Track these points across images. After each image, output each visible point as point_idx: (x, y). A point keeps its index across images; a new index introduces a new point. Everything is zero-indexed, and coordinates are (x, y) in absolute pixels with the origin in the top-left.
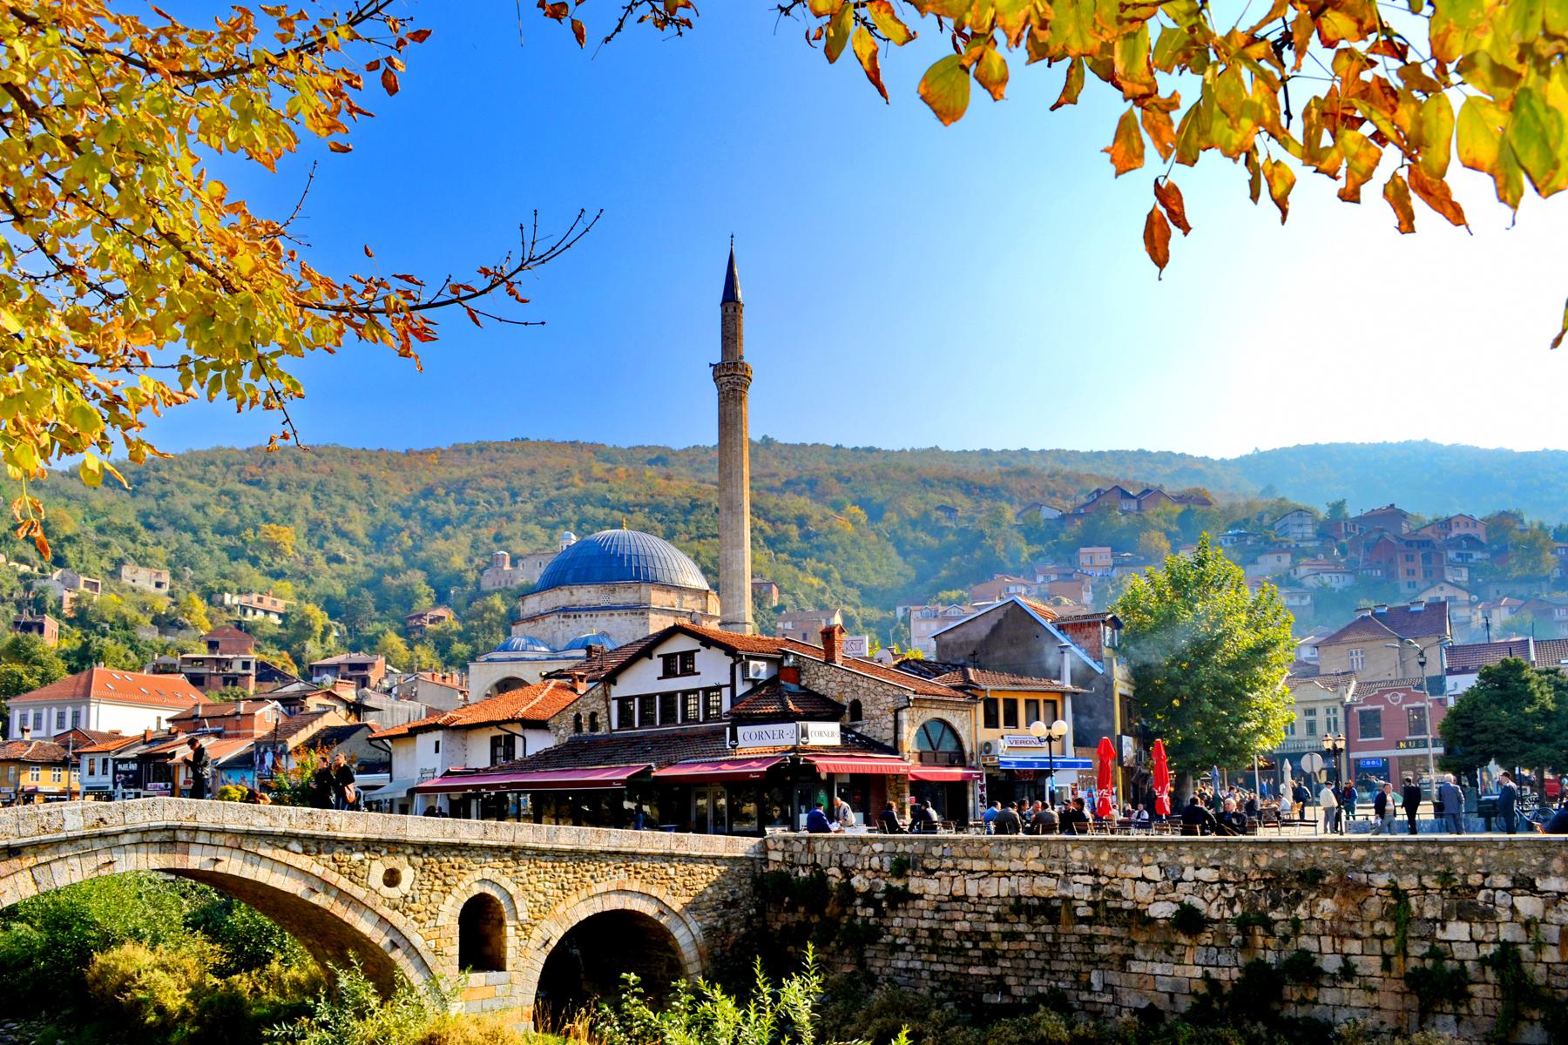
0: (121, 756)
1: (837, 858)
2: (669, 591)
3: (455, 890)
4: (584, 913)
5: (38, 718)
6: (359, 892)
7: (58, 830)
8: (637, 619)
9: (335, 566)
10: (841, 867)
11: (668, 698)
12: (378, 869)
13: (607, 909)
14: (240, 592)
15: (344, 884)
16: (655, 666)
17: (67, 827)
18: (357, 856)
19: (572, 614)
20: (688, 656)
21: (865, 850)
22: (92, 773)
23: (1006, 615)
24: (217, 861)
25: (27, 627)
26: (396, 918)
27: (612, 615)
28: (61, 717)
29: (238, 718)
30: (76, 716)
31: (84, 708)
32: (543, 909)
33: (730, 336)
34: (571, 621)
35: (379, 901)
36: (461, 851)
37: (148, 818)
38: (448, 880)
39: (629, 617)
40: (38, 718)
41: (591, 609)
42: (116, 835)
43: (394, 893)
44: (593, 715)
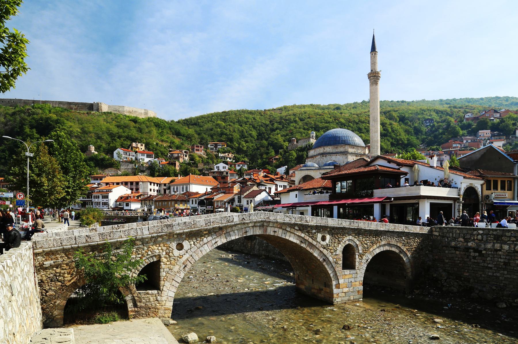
1: (462, 235)
2: (354, 148)
3: (341, 243)
4: (378, 251)
6: (314, 243)
7: (232, 222)
8: (344, 157)
10: (464, 238)
13: (384, 250)
15: (310, 240)
17: (234, 221)
18: (314, 231)
19: (324, 155)
21: (475, 232)
22: (192, 203)
24: (275, 232)
26: (325, 251)
32: (366, 250)
33: (373, 63)
34: (324, 158)
35: (320, 246)
36: (343, 230)
37: (256, 218)
38: (340, 239)
39: (342, 156)
42: (248, 224)
43: (323, 243)
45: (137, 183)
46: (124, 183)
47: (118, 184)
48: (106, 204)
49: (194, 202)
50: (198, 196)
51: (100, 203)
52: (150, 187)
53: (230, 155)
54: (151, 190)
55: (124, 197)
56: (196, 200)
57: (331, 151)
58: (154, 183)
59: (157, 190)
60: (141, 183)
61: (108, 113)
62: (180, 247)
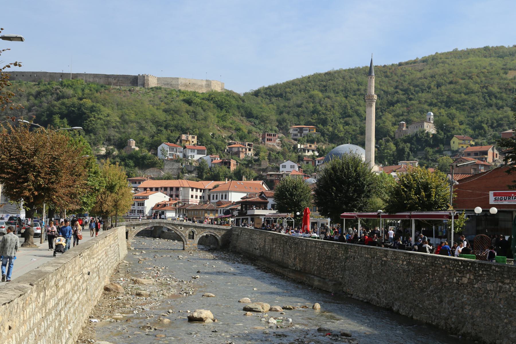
5: (217, 196)
12: (179, 227)
22: (220, 213)
26: (181, 232)
40: (217, 196)
45: (178, 189)
46: (163, 189)
47: (157, 189)
48: (141, 212)
51: (135, 210)
52: (191, 193)
53: (313, 146)
54: (192, 196)
55: (160, 204)
58: (197, 189)
59: (201, 197)
60: (181, 189)
61: (157, 88)
62: (134, 228)
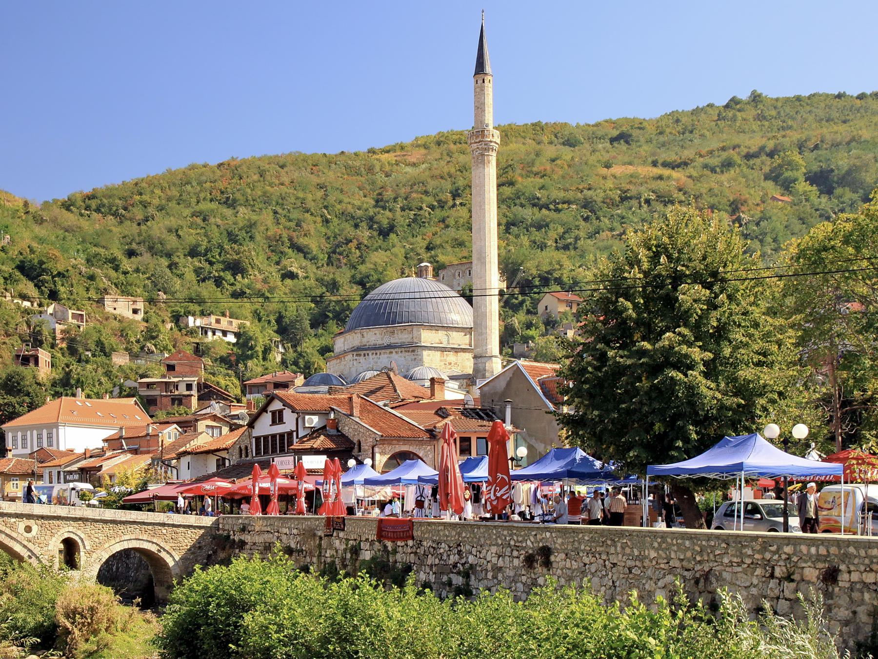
0: (68, 469)
3: (56, 535)
4: (118, 548)
5: (24, 439)
6: (14, 535)
9: (288, 281)
11: (274, 436)
12: (22, 525)
14: (203, 314)
15: (8, 531)
16: (267, 418)
18: (13, 520)
19: (362, 353)
20: (281, 412)
23: (513, 374)
25: (25, 360)
26: (30, 546)
27: (391, 353)
28: (40, 438)
29: (148, 438)
30: (50, 437)
31: (55, 430)
34: (362, 359)
35: (23, 538)
38: (53, 531)
39: (404, 354)
40: (24, 439)
41: (376, 348)
43: (29, 535)
44: (246, 448)
49: (55, 478)
50: (63, 461)
56: (59, 472)
57: (380, 342)
